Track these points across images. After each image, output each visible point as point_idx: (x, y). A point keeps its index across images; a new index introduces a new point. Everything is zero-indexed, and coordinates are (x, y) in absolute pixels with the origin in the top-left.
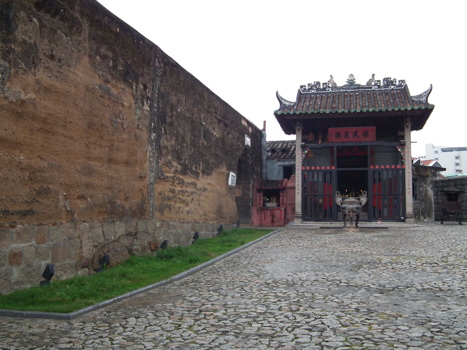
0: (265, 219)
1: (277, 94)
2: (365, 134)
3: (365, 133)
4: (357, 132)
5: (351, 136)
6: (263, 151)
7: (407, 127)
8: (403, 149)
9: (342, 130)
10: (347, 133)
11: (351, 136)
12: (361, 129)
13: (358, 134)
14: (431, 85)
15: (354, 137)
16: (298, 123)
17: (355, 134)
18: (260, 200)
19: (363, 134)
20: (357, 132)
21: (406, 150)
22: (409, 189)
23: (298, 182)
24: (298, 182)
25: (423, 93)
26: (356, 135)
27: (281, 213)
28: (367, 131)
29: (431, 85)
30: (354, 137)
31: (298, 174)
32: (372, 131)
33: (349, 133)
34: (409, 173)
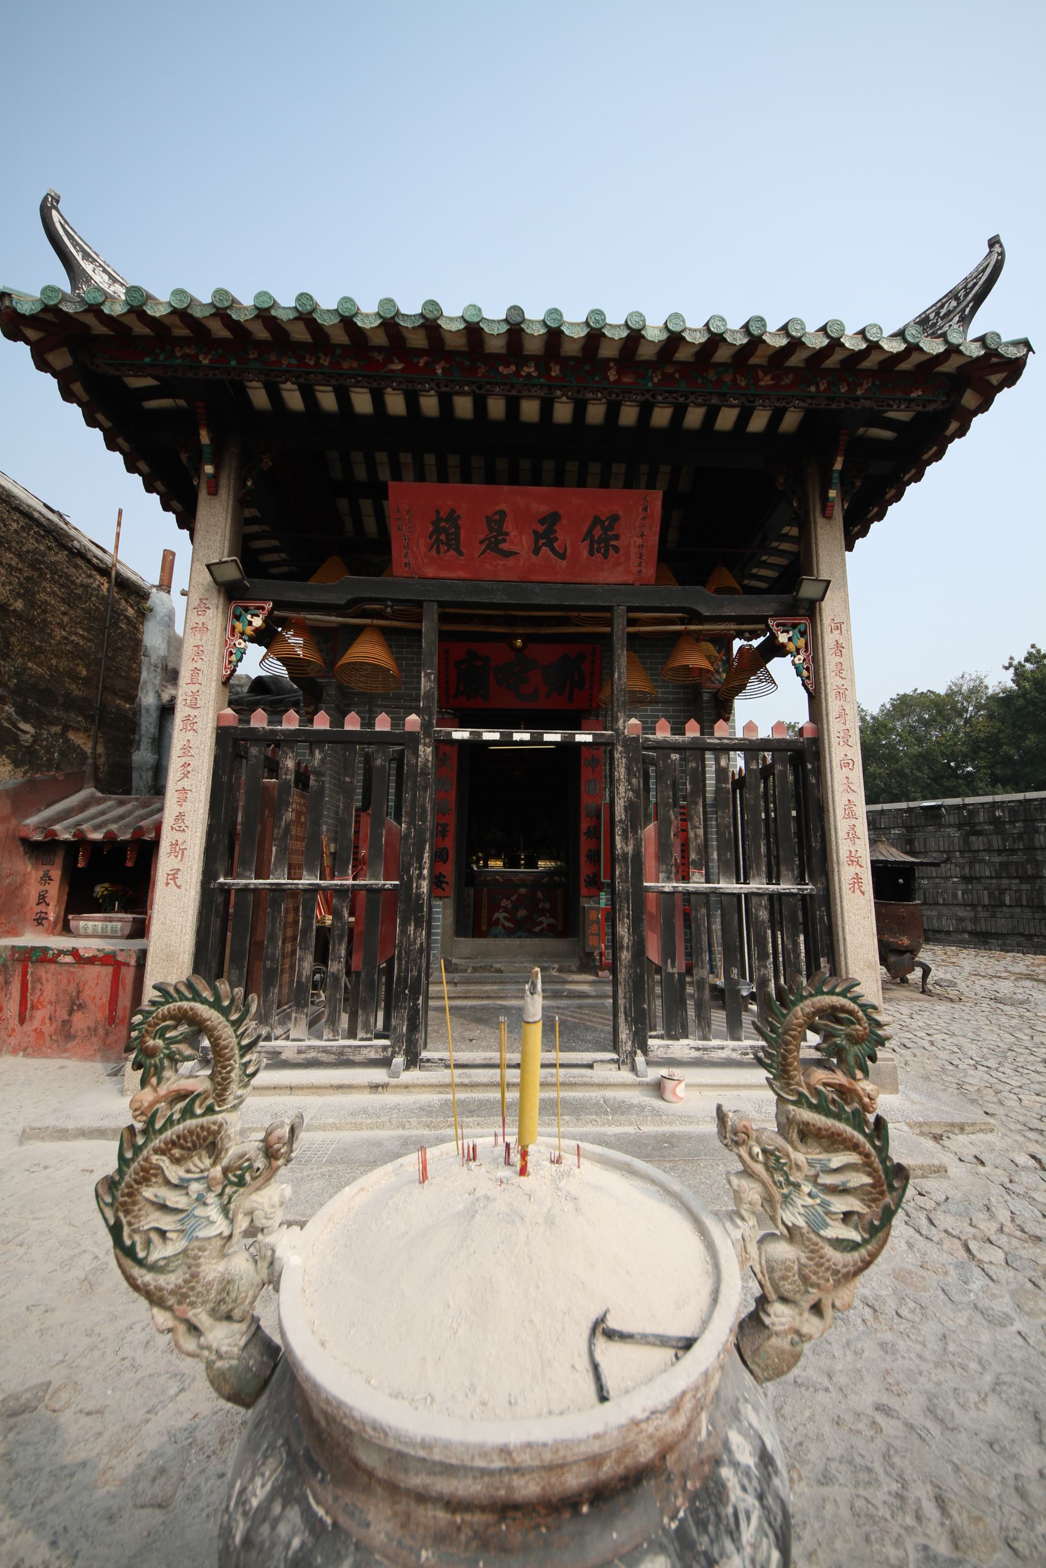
0: (22, 1020)
1: (46, 209)
2: (603, 538)
3: (598, 532)
4: (552, 519)
5: (519, 541)
6: (144, 675)
7: (828, 516)
8: (803, 634)
9: (470, 500)
10: (496, 524)
11: (519, 541)
12: (579, 504)
13: (563, 537)
14: (994, 242)
15: (536, 551)
16: (205, 438)
17: (546, 533)
18: (42, 899)
19: (589, 533)
20: (552, 519)
21: (829, 639)
22: (854, 860)
23: (182, 801)
24: (182, 801)
25: (941, 304)
26: (550, 544)
27: (116, 974)
28: (615, 518)
29: (994, 242)
30: (536, 551)
31: (186, 749)
32: (640, 518)
33: (509, 526)
34: (847, 764)
